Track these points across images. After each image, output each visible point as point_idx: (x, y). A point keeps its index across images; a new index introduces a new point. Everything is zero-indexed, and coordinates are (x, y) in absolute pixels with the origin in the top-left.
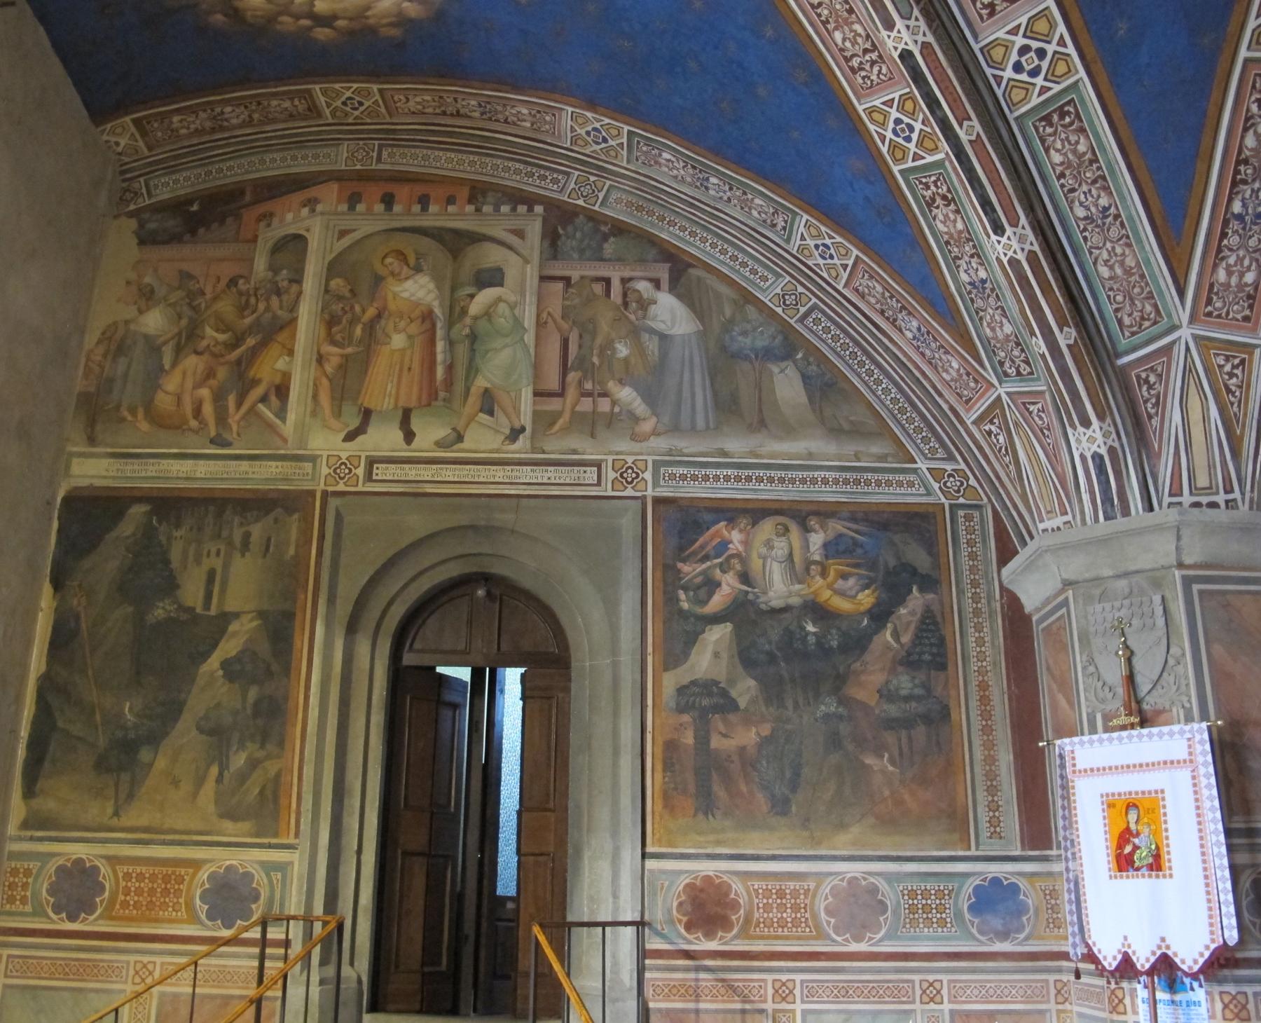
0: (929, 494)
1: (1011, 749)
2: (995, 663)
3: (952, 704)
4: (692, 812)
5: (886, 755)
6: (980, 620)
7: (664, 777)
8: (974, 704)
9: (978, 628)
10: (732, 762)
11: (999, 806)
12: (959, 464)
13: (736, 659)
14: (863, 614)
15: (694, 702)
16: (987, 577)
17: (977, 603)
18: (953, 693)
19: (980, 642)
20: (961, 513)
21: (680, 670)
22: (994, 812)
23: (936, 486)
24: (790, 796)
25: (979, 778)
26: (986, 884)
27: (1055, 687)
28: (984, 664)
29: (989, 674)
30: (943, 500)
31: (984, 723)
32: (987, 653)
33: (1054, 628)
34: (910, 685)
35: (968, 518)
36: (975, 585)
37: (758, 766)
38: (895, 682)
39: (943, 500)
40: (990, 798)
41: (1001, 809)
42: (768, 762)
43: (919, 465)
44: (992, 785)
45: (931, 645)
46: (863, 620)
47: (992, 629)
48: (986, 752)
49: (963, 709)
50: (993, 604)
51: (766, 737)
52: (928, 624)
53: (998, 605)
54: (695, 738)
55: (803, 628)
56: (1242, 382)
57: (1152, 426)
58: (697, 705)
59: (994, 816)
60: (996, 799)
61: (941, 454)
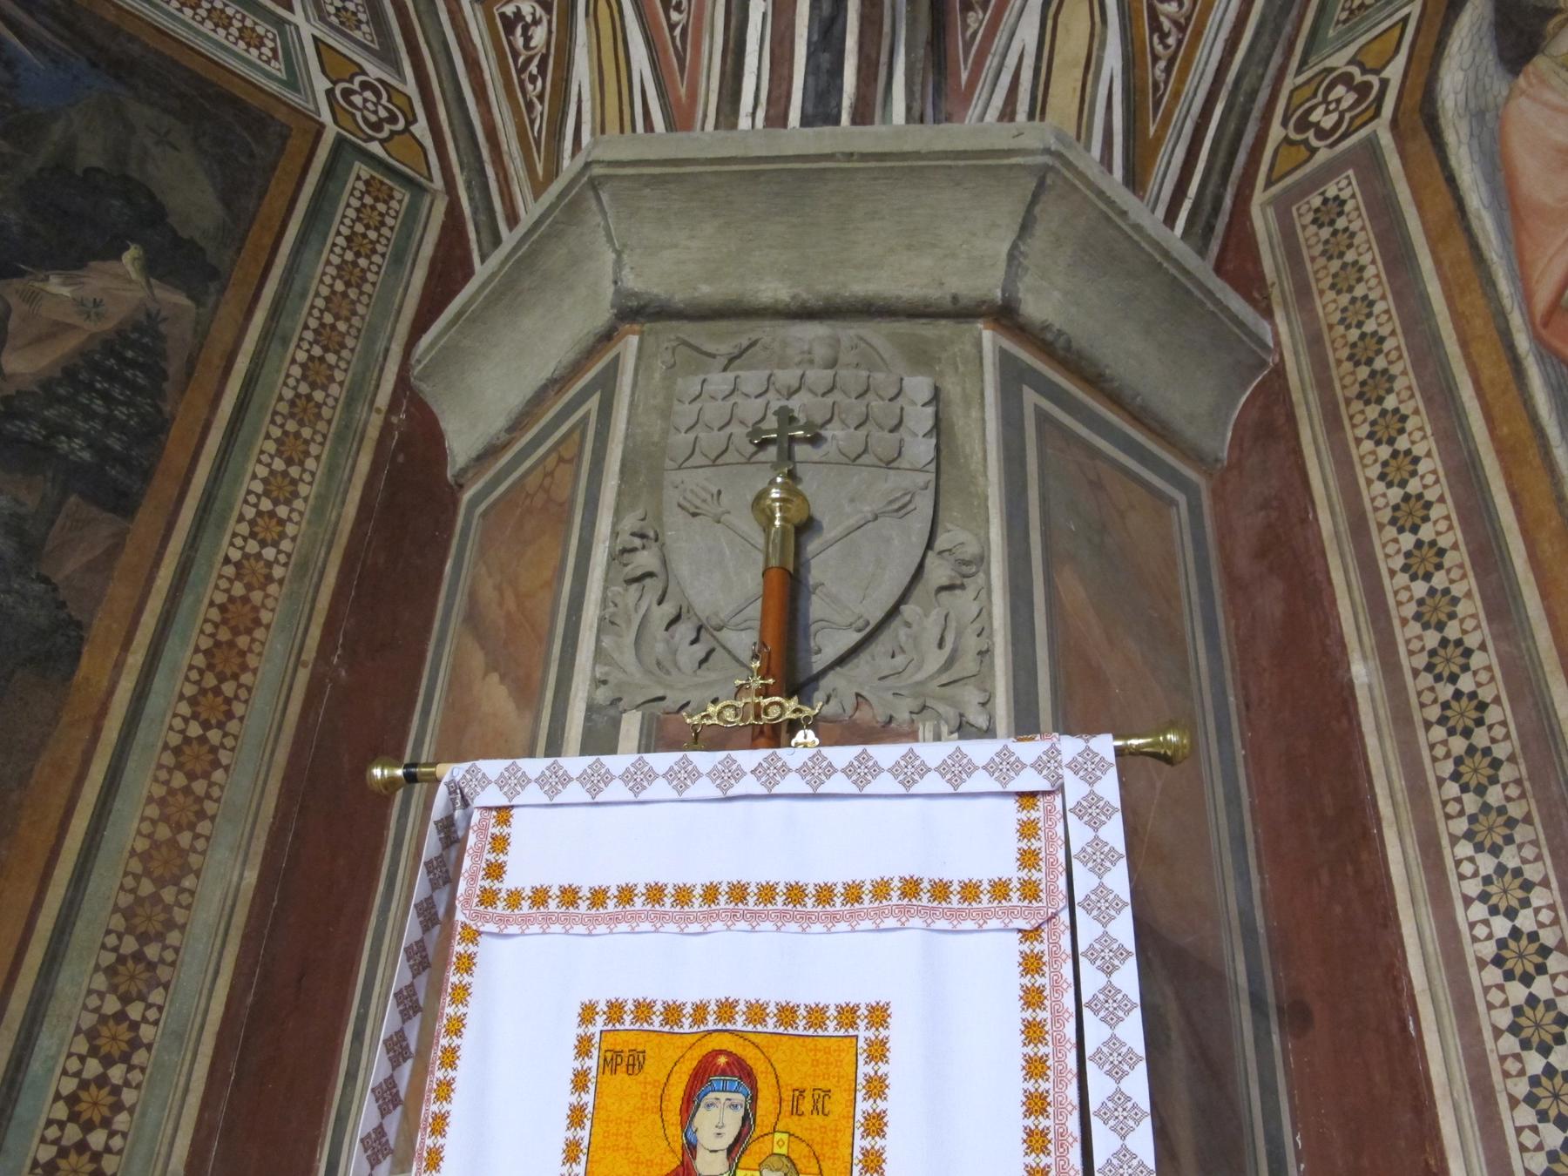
0: (292, 83)
1: (259, 845)
2: (303, 568)
3: (103, 627)
6: (306, 433)
8: (182, 654)
9: (292, 450)
12: (404, 80)
16: (371, 342)
17: (313, 386)
18: (120, 591)
19: (281, 488)
20: (362, 169)
23: (321, 84)
27: (477, 660)
28: (269, 553)
29: (273, 589)
30: (326, 116)
31: (195, 730)
32: (290, 529)
33: (532, 483)
36: (327, 337)
39: (326, 116)
40: (112, 1005)
43: (298, 18)
44: (138, 957)
45: (108, 421)
47: (331, 471)
48: (163, 832)
49: (136, 659)
50: (361, 411)
52: (132, 364)
53: (376, 421)
56: (1188, 19)
57: (965, 26)
60: (135, 1012)
61: (365, 33)
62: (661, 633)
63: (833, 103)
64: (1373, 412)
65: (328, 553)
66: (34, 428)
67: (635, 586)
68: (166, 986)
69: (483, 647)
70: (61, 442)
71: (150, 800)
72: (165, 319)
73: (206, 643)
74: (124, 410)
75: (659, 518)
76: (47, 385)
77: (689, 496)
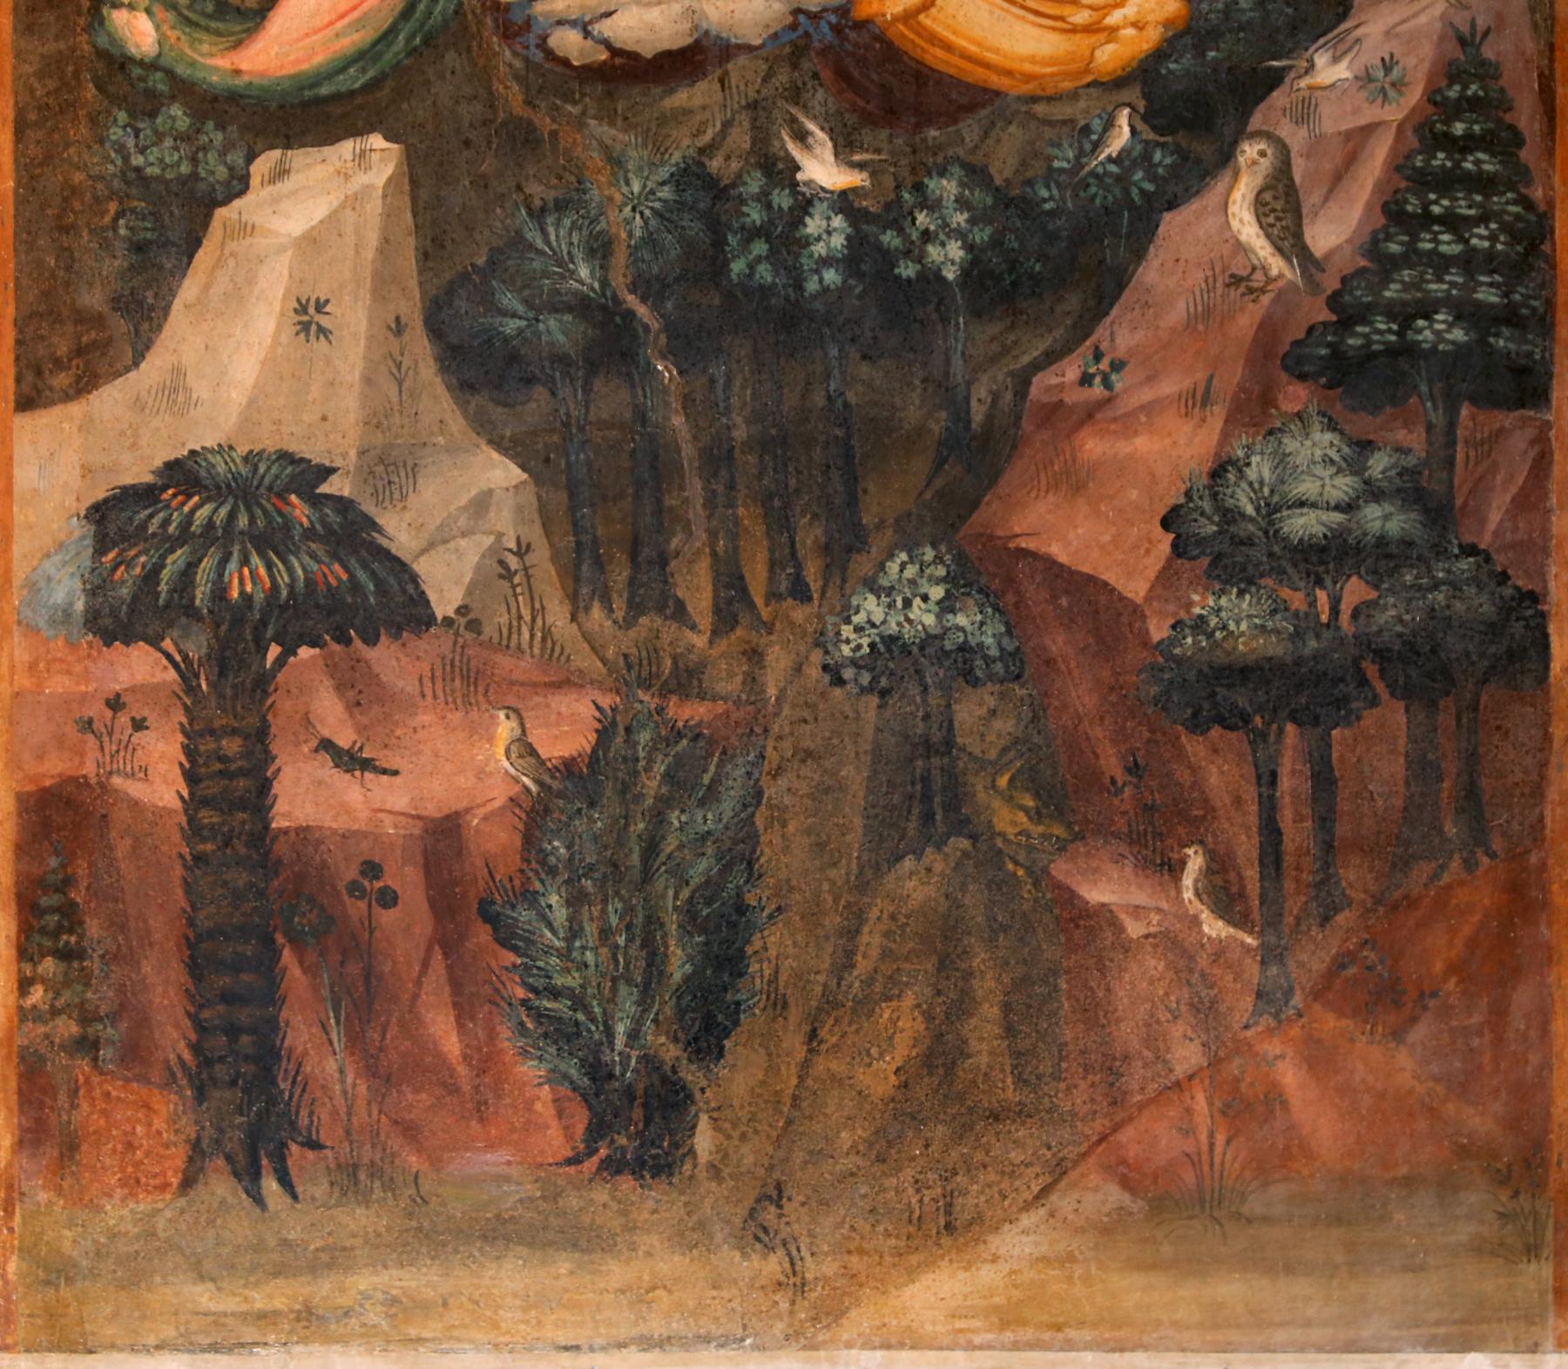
4: (178, 1157)
5: (1195, 861)
7: (24, 985)
10: (388, 899)
13: (421, 349)
14: (1118, 83)
15: (187, 576)
21: (110, 399)
24: (691, 1075)
34: (1342, 487)
37: (524, 915)
38: (1260, 468)
42: (576, 900)
45: (1469, 262)
46: (1109, 124)
51: (569, 765)
54: (191, 777)
55: (782, 172)
58: (201, 594)
66: (1382, 327)
70: (1420, 331)
72: (1486, 34)
74: (1482, 231)
76: (1373, 247)
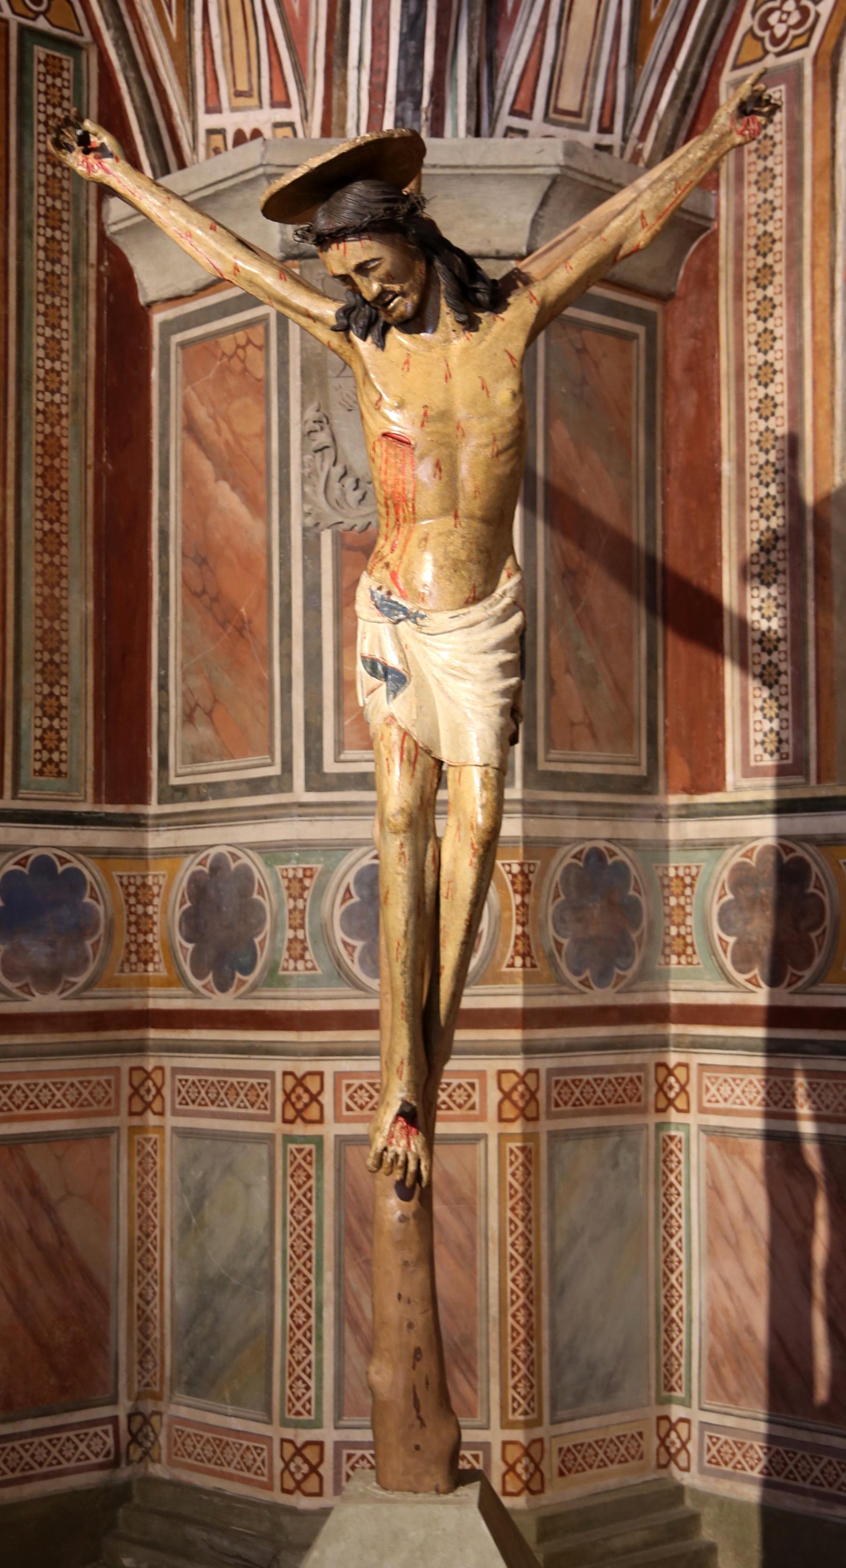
1: (90, 587)
2: (76, 401)
8: (31, 482)
11: (60, 707)
22: (51, 718)
25: (30, 644)
26: (26, 871)
27: (206, 467)
28: (57, 398)
29: (64, 422)
32: (64, 376)
33: (227, 344)
35: (53, 68)
41: (64, 714)
59: (51, 728)
62: (337, 486)
63: (418, 81)
64: (760, 295)
65: (86, 387)
67: (319, 454)
68: (66, 675)
69: (209, 458)
71: (37, 573)
73: (40, 470)
75: (327, 407)
77: (347, 399)
